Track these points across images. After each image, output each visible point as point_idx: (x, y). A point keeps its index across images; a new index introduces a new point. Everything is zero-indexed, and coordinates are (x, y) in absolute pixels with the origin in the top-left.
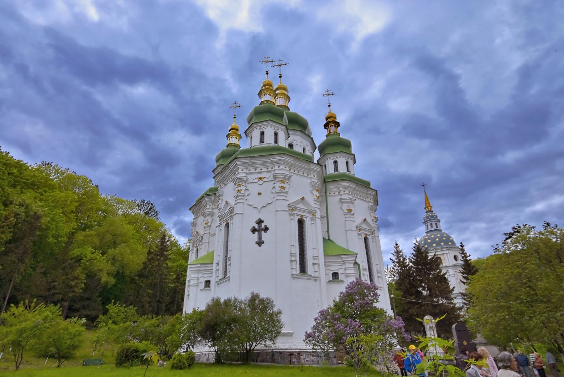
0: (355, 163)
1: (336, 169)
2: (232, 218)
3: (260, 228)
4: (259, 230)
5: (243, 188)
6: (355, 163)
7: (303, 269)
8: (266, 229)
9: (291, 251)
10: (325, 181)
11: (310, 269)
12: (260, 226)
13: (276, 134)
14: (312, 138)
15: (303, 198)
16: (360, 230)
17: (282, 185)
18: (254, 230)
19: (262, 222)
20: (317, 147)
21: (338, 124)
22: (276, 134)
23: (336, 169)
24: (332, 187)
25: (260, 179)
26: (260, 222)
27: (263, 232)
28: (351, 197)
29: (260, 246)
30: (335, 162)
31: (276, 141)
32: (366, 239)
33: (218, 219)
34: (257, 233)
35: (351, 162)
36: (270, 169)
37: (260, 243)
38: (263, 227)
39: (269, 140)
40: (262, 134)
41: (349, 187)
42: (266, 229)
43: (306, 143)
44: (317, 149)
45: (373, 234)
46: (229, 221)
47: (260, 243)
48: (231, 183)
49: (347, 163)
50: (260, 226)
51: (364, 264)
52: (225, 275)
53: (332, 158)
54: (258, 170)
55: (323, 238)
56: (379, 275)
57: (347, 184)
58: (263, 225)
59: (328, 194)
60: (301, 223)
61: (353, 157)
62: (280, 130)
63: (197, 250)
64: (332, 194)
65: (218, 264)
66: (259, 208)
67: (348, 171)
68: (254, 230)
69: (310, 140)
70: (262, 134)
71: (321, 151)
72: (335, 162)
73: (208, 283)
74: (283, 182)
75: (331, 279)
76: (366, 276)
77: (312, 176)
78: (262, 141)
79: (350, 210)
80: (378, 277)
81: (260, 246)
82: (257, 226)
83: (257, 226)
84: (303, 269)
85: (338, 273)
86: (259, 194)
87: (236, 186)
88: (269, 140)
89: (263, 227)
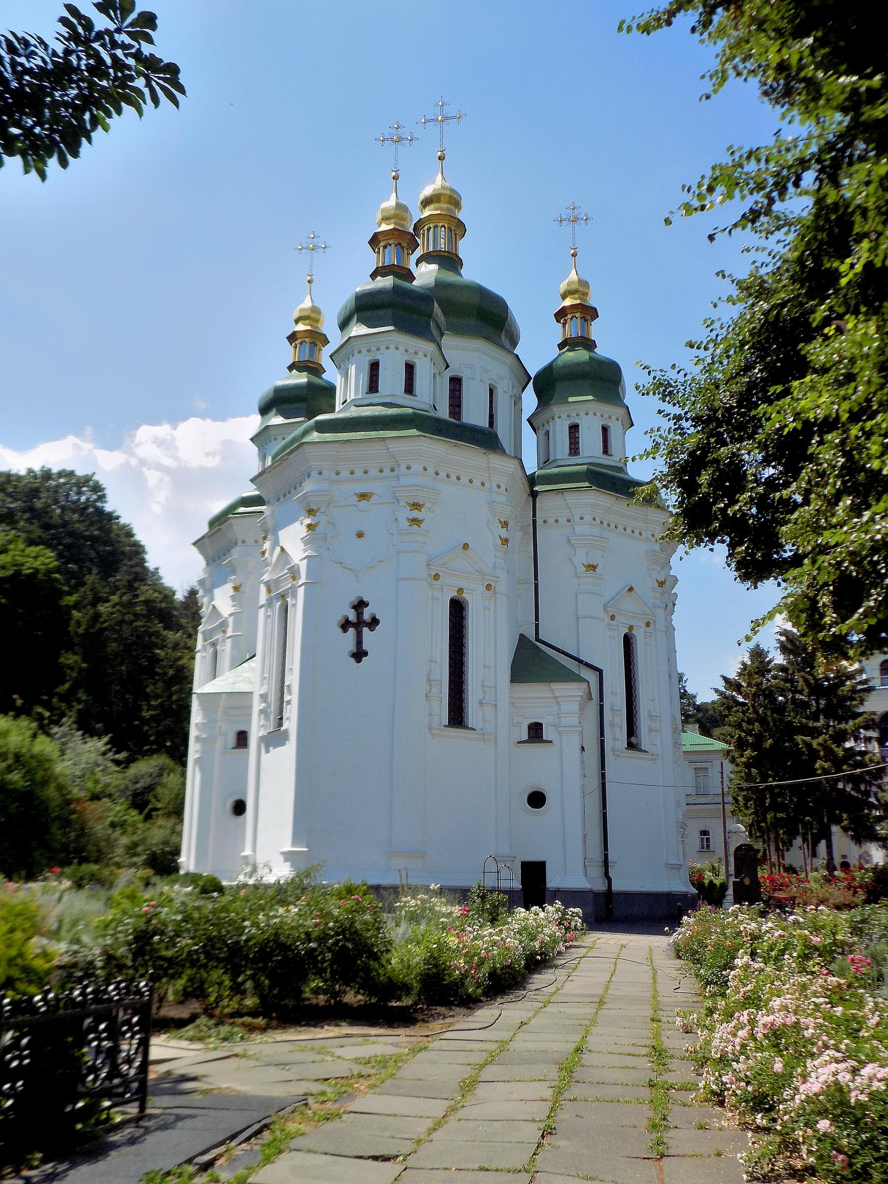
0: (632, 425)
1: (574, 449)
2: (293, 591)
3: (359, 621)
4: (359, 625)
5: (319, 517)
6: (632, 425)
7: (457, 716)
9: (429, 675)
10: (534, 495)
12: (359, 615)
13: (410, 369)
14: (517, 356)
15: (466, 546)
16: (613, 618)
17: (415, 514)
18: (345, 625)
19: (367, 605)
21: (589, 313)
22: (410, 369)
23: (574, 449)
24: (550, 505)
25: (364, 496)
26: (360, 605)
27: (365, 630)
28: (596, 531)
30: (574, 429)
31: (409, 388)
32: (628, 641)
33: (263, 589)
36: (387, 471)
37: (359, 655)
38: (366, 616)
39: (392, 381)
40: (374, 366)
45: (648, 624)
47: (359, 655)
49: (605, 430)
50: (359, 615)
52: (280, 724)
53: (564, 416)
54: (359, 473)
55: (522, 637)
58: (367, 615)
61: (622, 411)
62: (421, 354)
63: (215, 654)
64: (551, 521)
65: (264, 697)
67: (606, 450)
68: (345, 625)
69: (510, 359)
70: (374, 366)
71: (539, 392)
72: (574, 429)
73: (242, 739)
74: (416, 506)
75: (525, 737)
76: (617, 729)
78: (373, 387)
79: (592, 567)
80: (651, 730)
82: (352, 617)
83: (352, 616)
84: (457, 716)
85: (541, 725)
86: (360, 535)
88: (392, 381)
89: (366, 616)
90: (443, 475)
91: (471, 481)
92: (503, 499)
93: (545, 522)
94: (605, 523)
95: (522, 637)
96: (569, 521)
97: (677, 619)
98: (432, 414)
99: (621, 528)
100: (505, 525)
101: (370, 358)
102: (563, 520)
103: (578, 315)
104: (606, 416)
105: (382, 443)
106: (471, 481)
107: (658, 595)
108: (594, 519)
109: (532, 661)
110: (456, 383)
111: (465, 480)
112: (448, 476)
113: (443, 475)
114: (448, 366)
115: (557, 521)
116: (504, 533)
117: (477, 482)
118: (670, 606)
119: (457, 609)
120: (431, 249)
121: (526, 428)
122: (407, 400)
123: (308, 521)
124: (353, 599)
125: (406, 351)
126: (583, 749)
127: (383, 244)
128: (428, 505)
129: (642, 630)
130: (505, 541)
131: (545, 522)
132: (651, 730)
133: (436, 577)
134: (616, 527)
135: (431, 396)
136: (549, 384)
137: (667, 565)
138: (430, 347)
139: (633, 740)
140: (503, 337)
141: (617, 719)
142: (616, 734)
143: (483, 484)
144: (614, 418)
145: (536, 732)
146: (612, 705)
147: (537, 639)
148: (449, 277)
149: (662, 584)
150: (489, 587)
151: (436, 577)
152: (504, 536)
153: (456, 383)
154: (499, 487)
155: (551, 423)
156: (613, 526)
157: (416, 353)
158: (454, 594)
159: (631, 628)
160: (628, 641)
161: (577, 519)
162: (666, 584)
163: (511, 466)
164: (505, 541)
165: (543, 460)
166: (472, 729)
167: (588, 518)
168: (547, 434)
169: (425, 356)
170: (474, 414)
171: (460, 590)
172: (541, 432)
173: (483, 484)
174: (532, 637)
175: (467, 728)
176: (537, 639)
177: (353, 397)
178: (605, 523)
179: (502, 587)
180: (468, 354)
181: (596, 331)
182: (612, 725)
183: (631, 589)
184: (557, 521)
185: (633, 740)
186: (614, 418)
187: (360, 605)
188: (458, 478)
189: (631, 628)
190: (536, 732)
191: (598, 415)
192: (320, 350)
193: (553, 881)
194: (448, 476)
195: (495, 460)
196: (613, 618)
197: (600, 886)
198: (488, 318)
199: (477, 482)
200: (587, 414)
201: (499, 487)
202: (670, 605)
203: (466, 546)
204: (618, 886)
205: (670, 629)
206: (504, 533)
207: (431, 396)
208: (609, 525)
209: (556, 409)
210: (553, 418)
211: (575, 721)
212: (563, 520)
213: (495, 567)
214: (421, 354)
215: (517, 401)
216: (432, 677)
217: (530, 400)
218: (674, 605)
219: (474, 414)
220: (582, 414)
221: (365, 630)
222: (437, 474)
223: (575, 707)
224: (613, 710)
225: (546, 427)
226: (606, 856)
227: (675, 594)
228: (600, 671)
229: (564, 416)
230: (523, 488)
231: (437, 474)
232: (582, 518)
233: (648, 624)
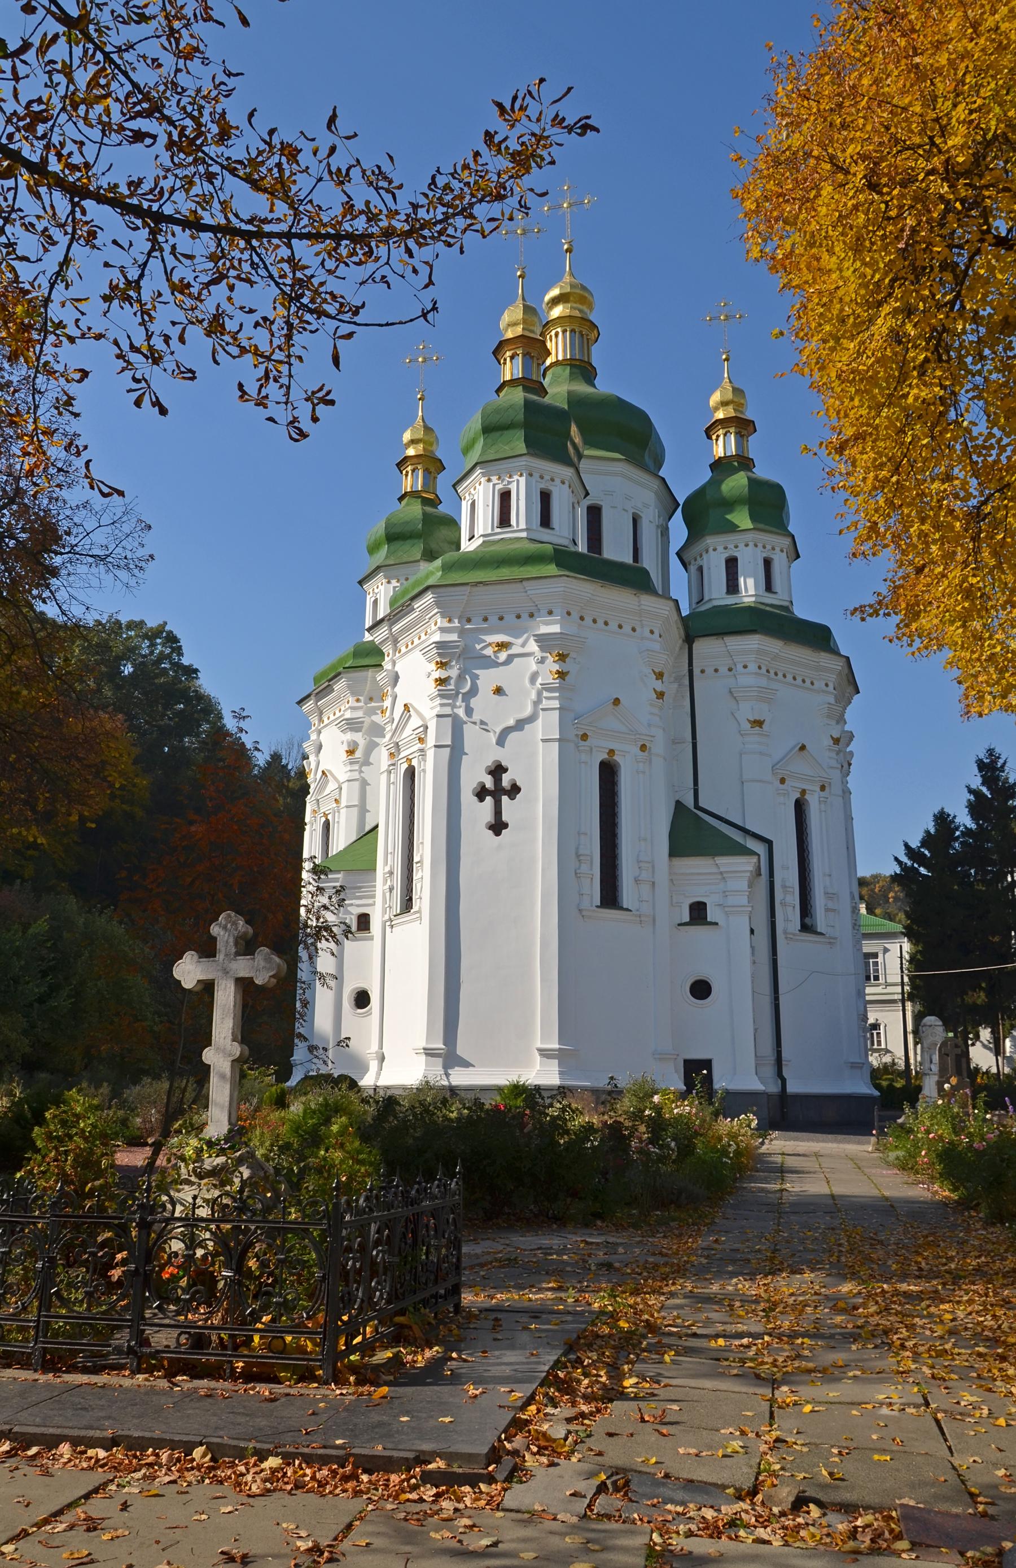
0: (798, 556)
6: (798, 556)
8: (514, 790)
9: (577, 849)
10: (689, 640)
11: (628, 893)
12: (497, 780)
14: (663, 479)
15: (617, 702)
16: (783, 781)
20: (681, 503)
22: (545, 497)
23: (733, 587)
26: (497, 771)
27: (505, 799)
28: (763, 682)
29: (498, 833)
30: (732, 564)
31: (546, 521)
32: (800, 807)
34: (489, 799)
35: (779, 561)
37: (498, 827)
40: (505, 497)
41: (759, 652)
42: (514, 790)
43: (644, 497)
44: (680, 509)
46: (415, 763)
47: (498, 827)
48: (417, 654)
49: (768, 563)
50: (497, 780)
51: (787, 874)
53: (720, 549)
55: (679, 804)
56: (830, 905)
57: (754, 642)
58: (506, 780)
59: (696, 671)
60: (608, 773)
61: (786, 542)
62: (558, 481)
63: (327, 826)
64: (710, 671)
66: (498, 730)
67: (769, 587)
69: (655, 484)
70: (505, 497)
71: (689, 520)
75: (686, 918)
76: (790, 909)
77: (647, 634)
79: (759, 723)
81: (498, 833)
82: (489, 783)
83: (489, 783)
87: (433, 666)
90: (588, 620)
91: (620, 627)
92: (657, 646)
93: (703, 671)
94: (772, 672)
95: (679, 804)
96: (730, 670)
97: (852, 781)
98: (572, 549)
99: (790, 677)
100: (660, 676)
101: (500, 486)
102: (723, 670)
103: (732, 430)
104: (769, 547)
105: (519, 585)
106: (620, 627)
107: (834, 755)
108: (760, 668)
109: (694, 832)
110: (594, 514)
111: (613, 625)
112: (595, 621)
113: (588, 620)
114: (587, 494)
115: (716, 671)
116: (659, 686)
117: (627, 629)
118: (845, 768)
119: (608, 773)
120: (560, 358)
121: (674, 562)
122: (545, 535)
123: (437, 674)
124: (489, 762)
125: (542, 477)
126: (752, 931)
127: (508, 354)
128: (573, 655)
129: (816, 796)
130: (660, 695)
131: (703, 671)
132: (827, 910)
133: (584, 737)
134: (784, 676)
135: (569, 529)
136: (703, 513)
137: (841, 720)
138: (568, 472)
139: (807, 920)
140: (646, 458)
141: (789, 899)
142: (789, 916)
143: (634, 630)
144: (778, 549)
145: (698, 913)
146: (783, 880)
147: (697, 806)
148: (582, 388)
149: (836, 741)
150: (643, 748)
151: (584, 737)
152: (659, 689)
153: (594, 514)
154: (652, 632)
155: (705, 556)
156: (780, 675)
157: (552, 480)
158: (606, 756)
159: (803, 792)
160: (800, 807)
161: (740, 667)
162: (841, 741)
163: (665, 608)
164: (660, 695)
165: (695, 600)
166: (627, 910)
167: (752, 667)
168: (700, 569)
169: (563, 483)
170: (616, 549)
171: (611, 752)
172: (693, 568)
173: (634, 630)
174: (689, 802)
175: (622, 908)
176: (697, 806)
177: (481, 532)
178: (772, 672)
179: (659, 747)
180: (611, 480)
181: (754, 447)
182: (784, 904)
183: (803, 748)
184: (716, 671)
185: (807, 920)
186: (778, 549)
187: (497, 771)
188: (606, 623)
189: (803, 792)
190: (698, 913)
191: (760, 545)
192: (435, 478)
193: (721, 1083)
194: (595, 621)
195: (647, 601)
196: (783, 781)
197: (774, 1088)
198: (629, 434)
199: (627, 629)
200: (747, 545)
201: (652, 632)
202: (846, 766)
203: (617, 702)
204: (792, 1088)
205: (846, 793)
206: (659, 686)
207: (569, 529)
208: (776, 674)
209: (710, 541)
210: (707, 551)
211: (744, 900)
212: (723, 670)
213: (649, 725)
214: (558, 481)
215: (664, 532)
216: (581, 852)
217: (678, 530)
218: (850, 764)
219: (616, 549)
220: (741, 546)
221: (505, 799)
222: (582, 618)
223: (744, 885)
224: (784, 887)
225: (699, 562)
226: (779, 1054)
227: (851, 753)
228: (769, 843)
229: (720, 549)
230: (677, 634)
231: (582, 618)
232: (745, 667)
233: (823, 788)
